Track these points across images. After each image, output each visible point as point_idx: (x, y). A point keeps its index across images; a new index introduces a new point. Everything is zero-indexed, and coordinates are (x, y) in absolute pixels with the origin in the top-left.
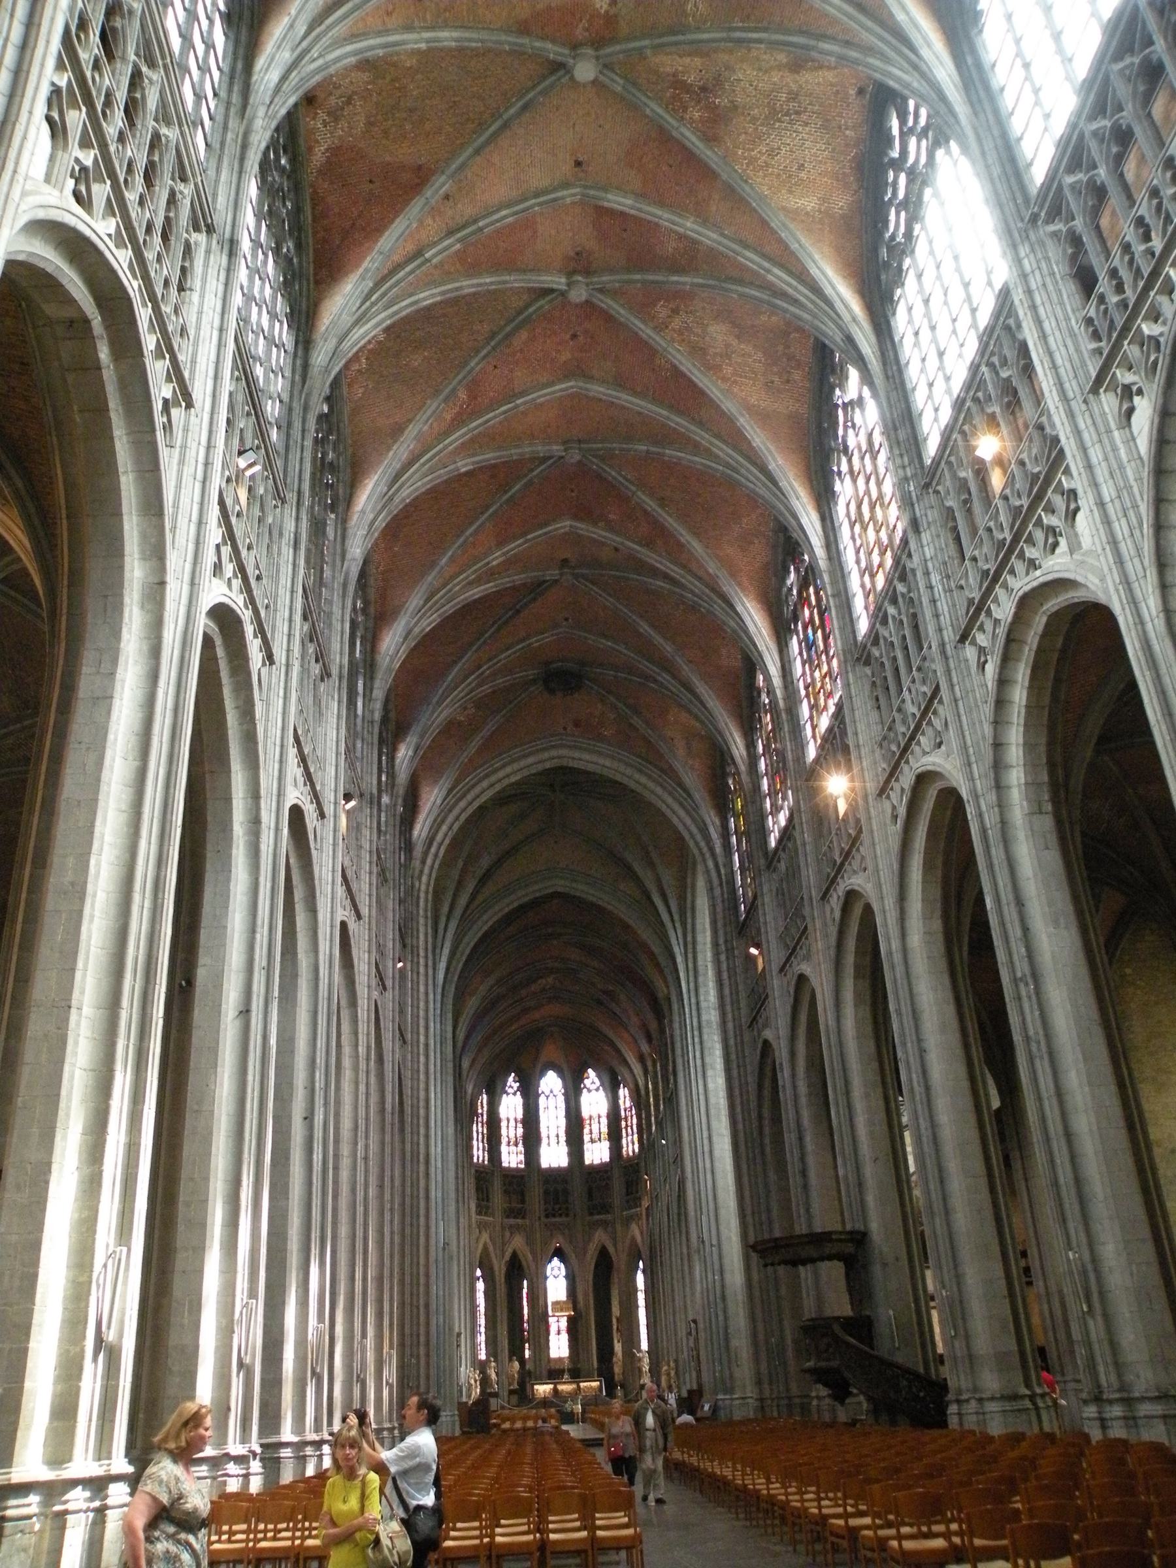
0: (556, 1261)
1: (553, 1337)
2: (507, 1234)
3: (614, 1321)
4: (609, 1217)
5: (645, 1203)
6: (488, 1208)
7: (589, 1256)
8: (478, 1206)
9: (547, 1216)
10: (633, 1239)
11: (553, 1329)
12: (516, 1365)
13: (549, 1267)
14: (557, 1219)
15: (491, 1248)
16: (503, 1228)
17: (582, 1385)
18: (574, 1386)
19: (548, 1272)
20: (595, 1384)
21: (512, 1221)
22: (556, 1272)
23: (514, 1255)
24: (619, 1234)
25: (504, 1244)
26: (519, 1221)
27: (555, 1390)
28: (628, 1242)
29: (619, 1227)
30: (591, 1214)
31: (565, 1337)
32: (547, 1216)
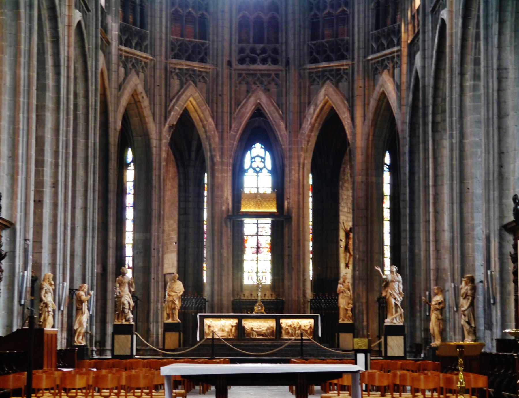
0: (258, 149)
1: (249, 255)
2: (176, 83)
3: (342, 235)
4: (344, 64)
5: (406, 37)
6: (142, 38)
7: (307, 126)
8: (123, 30)
9: (242, 61)
10: (383, 97)
11: (250, 243)
12: (179, 287)
13: (248, 157)
14: (259, 66)
15: (145, 103)
16: (168, 73)
17: (285, 323)
18: (272, 323)
19: (247, 164)
20: (307, 323)
21: (184, 64)
22: (258, 163)
23: (185, 113)
24: (358, 91)
25: (168, 99)
26: (196, 65)
27: (240, 327)
28: (373, 104)
29: (359, 82)
30: (315, 61)
31: (266, 256)
32: (242, 61)
